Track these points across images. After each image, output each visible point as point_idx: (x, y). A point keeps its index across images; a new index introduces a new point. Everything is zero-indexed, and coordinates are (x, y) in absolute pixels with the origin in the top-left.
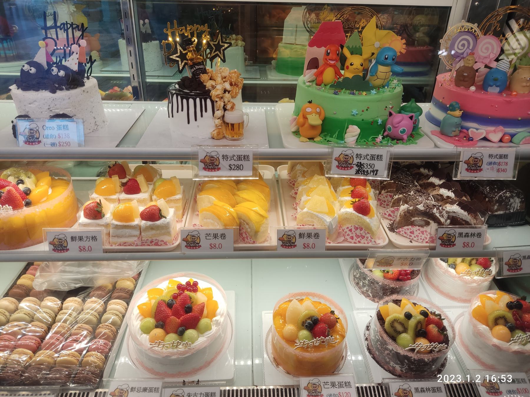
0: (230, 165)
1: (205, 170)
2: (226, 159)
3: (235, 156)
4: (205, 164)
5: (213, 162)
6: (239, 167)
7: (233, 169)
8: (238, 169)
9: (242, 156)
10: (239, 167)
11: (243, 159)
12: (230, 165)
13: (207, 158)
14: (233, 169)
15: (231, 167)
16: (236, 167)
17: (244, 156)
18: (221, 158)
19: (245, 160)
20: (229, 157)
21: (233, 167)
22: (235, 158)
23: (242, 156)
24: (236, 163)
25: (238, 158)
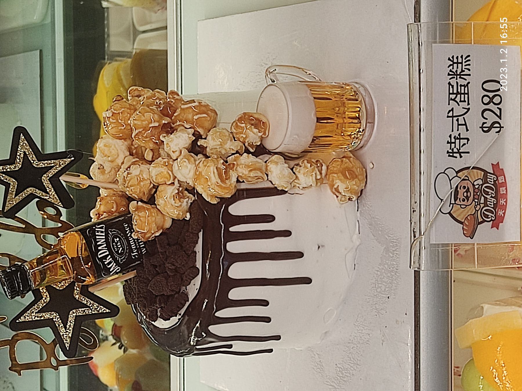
0: (482, 127)
1: (501, 219)
2: (463, 142)
3: (452, 109)
4: (480, 220)
5: (471, 190)
6: (491, 95)
7: (498, 120)
8: (497, 100)
9: (453, 82)
10: (491, 95)
11: (461, 82)
12: (482, 127)
13: (461, 214)
14: (498, 120)
15: (492, 126)
16: (491, 106)
17: (453, 74)
18: (458, 163)
19: (467, 72)
20: (455, 133)
21: (491, 118)
22: (459, 110)
23: (453, 82)
24: (476, 106)
25: (458, 99)
